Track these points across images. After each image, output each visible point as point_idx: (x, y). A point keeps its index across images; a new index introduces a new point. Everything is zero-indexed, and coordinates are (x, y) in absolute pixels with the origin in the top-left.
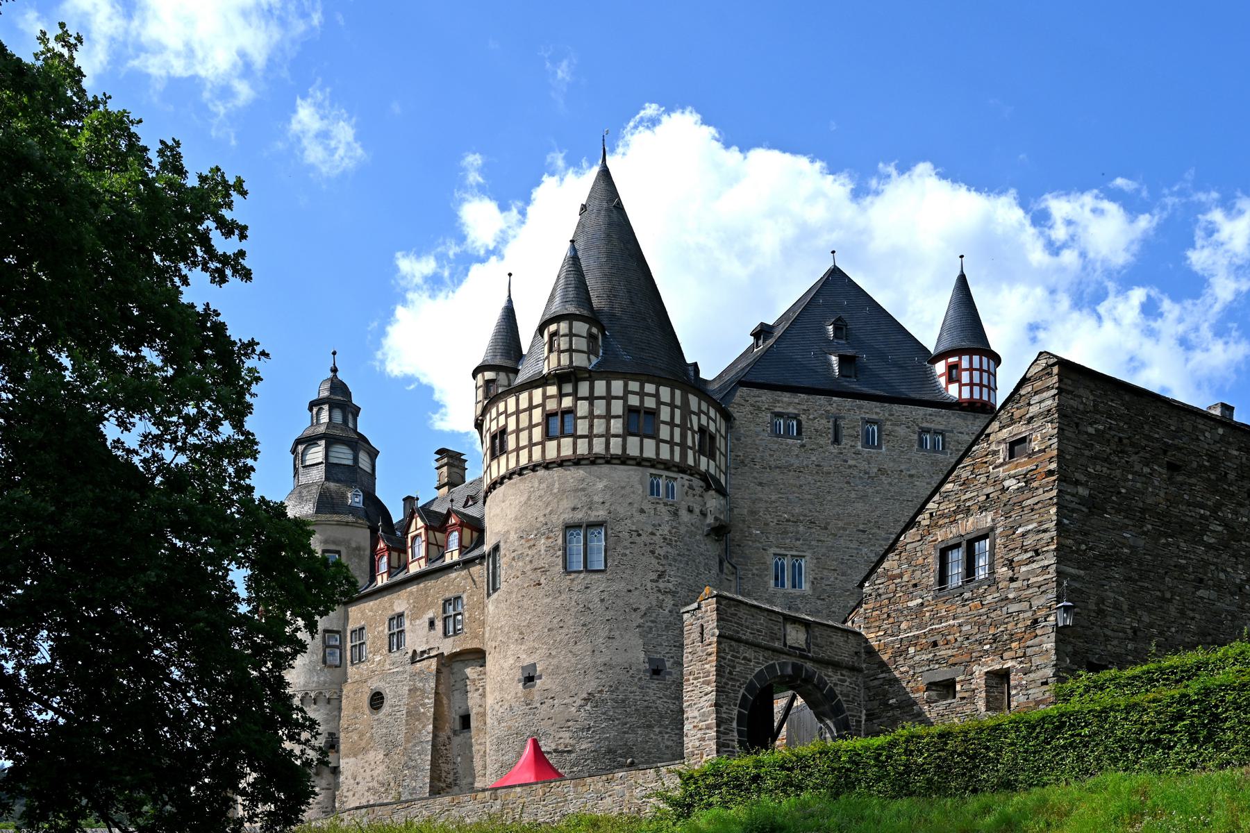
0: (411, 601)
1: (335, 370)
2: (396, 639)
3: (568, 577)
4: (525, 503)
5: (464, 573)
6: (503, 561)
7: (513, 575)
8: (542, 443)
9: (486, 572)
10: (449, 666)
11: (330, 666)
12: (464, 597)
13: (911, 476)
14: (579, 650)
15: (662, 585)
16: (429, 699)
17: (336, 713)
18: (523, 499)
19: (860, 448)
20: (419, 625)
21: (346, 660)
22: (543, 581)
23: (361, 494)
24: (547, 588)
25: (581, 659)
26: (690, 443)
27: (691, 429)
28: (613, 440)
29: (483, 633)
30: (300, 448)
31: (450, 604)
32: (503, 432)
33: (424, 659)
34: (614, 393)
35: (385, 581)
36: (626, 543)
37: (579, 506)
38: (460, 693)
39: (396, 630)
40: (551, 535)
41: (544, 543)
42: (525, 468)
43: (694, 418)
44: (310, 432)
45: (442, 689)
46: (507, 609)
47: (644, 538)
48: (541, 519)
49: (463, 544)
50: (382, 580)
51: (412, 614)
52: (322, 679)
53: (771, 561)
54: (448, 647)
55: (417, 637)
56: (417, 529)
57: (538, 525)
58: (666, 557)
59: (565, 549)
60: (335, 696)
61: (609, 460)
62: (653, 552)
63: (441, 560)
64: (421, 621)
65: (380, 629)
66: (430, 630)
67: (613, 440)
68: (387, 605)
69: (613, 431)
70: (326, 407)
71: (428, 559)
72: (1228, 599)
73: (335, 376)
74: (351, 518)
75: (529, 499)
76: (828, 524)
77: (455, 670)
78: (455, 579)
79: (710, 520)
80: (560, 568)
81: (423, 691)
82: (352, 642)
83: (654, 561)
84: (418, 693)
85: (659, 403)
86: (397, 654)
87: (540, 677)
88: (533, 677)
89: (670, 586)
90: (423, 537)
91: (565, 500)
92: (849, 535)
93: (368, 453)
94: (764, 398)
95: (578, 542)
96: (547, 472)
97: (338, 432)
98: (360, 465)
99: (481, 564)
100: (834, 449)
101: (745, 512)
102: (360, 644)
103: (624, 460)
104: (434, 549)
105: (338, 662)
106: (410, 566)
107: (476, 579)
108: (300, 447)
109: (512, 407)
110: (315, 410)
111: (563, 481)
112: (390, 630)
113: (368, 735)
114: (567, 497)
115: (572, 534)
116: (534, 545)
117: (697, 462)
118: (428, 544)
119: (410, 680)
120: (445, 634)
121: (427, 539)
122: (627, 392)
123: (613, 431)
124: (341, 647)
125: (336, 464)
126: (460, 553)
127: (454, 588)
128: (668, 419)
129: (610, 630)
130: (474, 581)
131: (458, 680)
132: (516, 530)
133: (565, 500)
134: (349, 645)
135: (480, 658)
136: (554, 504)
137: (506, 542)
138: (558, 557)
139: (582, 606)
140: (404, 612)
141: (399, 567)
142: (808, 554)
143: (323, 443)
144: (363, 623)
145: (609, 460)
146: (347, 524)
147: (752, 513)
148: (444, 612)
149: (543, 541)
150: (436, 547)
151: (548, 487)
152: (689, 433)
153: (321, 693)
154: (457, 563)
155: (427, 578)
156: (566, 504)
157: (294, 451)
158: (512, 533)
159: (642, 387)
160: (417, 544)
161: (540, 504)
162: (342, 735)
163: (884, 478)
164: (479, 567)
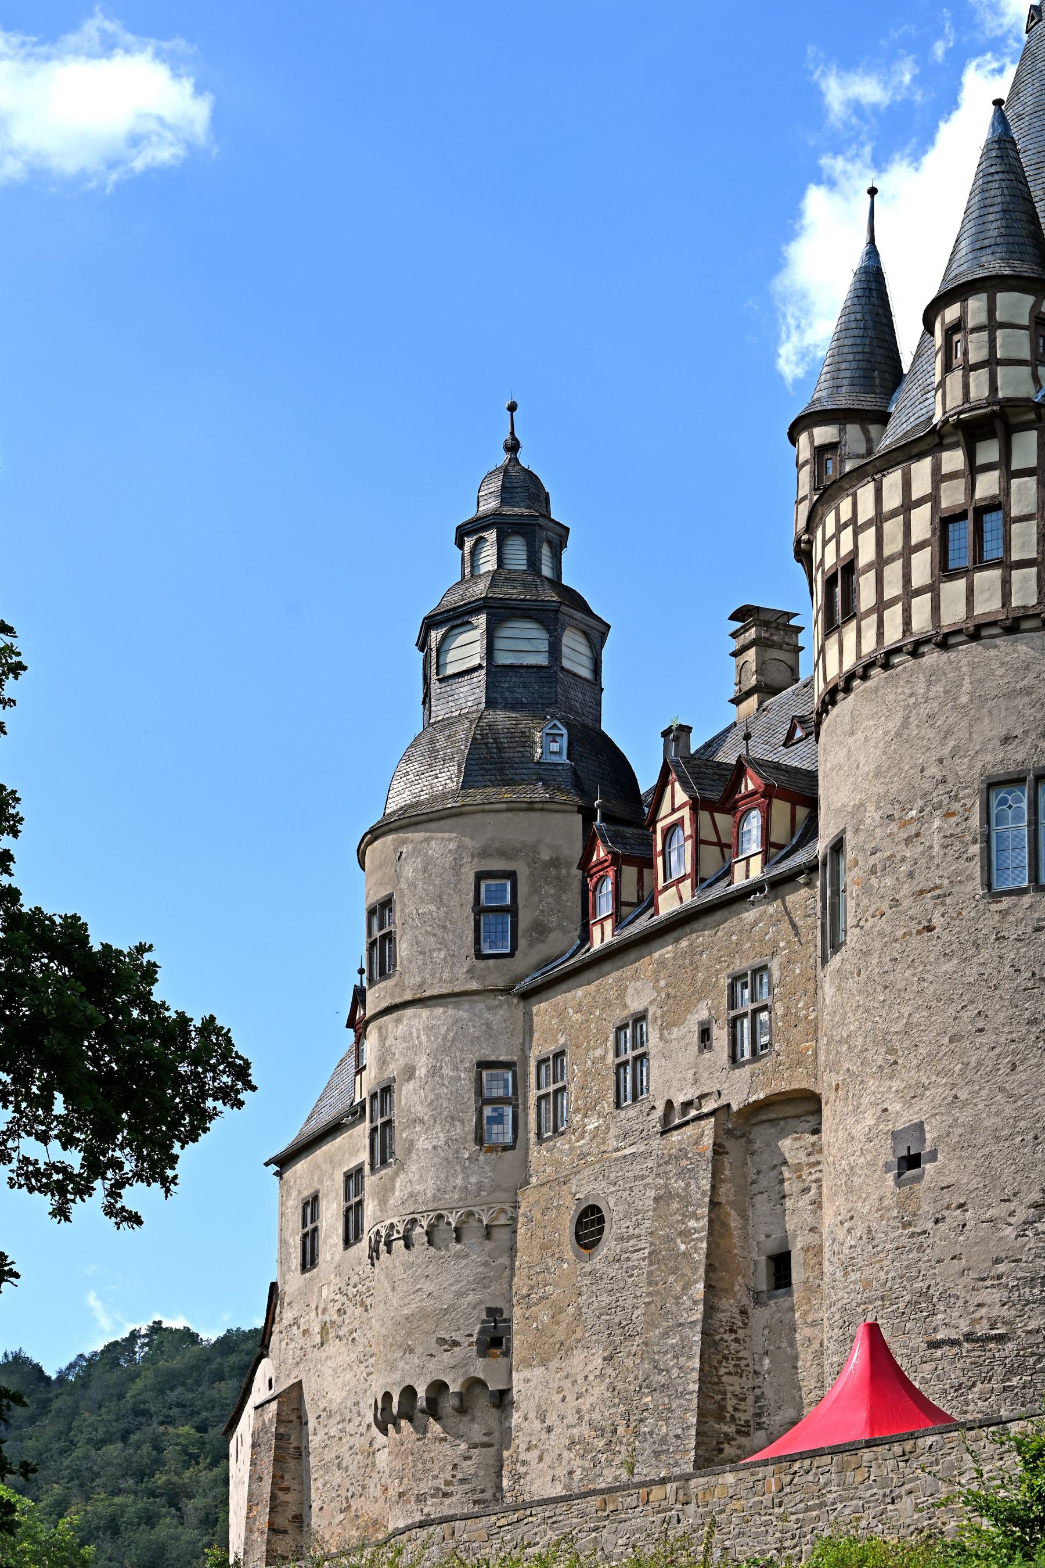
0: (662, 983)
1: (513, 447)
3: (994, 907)
4: (898, 734)
5: (773, 908)
6: (850, 878)
7: (872, 909)
8: (933, 589)
9: (819, 905)
10: (743, 1135)
11: (491, 1149)
12: (775, 965)
14: (1021, 1084)
16: (698, 1219)
17: (504, 1260)
18: (893, 725)
20: (678, 1040)
21: (527, 1131)
22: (937, 921)
23: (564, 731)
24: (946, 936)
25: (1027, 1107)
29: (816, 1053)
30: (435, 636)
31: (745, 986)
32: (849, 568)
33: (687, 1123)
35: (608, 938)
37: (1019, 732)
38: (769, 1201)
39: (630, 1054)
40: (956, 806)
41: (940, 829)
42: (897, 651)
44: (455, 599)
45: (726, 1191)
46: (860, 992)
48: (933, 770)
49: (773, 839)
50: (603, 936)
51: (664, 1014)
52: (473, 1180)
56: (674, 810)
57: (927, 785)
59: (987, 840)
60: (503, 1220)
63: (725, 882)
64: (684, 1030)
65: (598, 1052)
66: (701, 1051)
68: (612, 994)
70: (491, 536)
71: (699, 881)
73: (515, 461)
74: (540, 793)
75: (906, 723)
77: (757, 1146)
78: (755, 923)
81: (686, 1200)
82: (539, 1088)
84: (675, 1206)
86: (632, 1113)
87: (933, 1156)
88: (918, 1155)
90: (688, 830)
91: (987, 721)
93: (584, 633)
95: (1018, 818)
96: (945, 656)
97: (515, 592)
98: (566, 664)
99: (809, 884)
102: (556, 1092)
104: (710, 854)
105: (508, 1138)
106: (661, 899)
107: (799, 923)
108: (433, 633)
109: (866, 511)
110: (469, 543)
111: (980, 673)
112: (617, 1054)
113: (571, 1310)
114: (990, 712)
115: (1003, 801)
116: (918, 835)
118: (698, 842)
119: (658, 1175)
120: (734, 1059)
121: (697, 831)
124: (514, 1101)
125: (512, 667)
126: (765, 862)
127: (752, 947)
130: (794, 926)
131: (764, 1167)
132: (878, 802)
133: (987, 721)
134: (533, 1094)
135: (812, 1113)
136: (961, 733)
137: (857, 831)
138: (970, 859)
139: (1029, 974)
140: (646, 1010)
141: (640, 900)
143: (481, 620)
144: (562, 1041)
146: (531, 807)
148: (732, 1005)
149: (937, 823)
150: (717, 848)
151: (946, 692)
153: (471, 1214)
154: (756, 888)
155: (696, 925)
156: (989, 729)
157: (423, 644)
158: (871, 807)
160: (674, 845)
161: (931, 733)
162: (517, 1311)
164: (804, 892)
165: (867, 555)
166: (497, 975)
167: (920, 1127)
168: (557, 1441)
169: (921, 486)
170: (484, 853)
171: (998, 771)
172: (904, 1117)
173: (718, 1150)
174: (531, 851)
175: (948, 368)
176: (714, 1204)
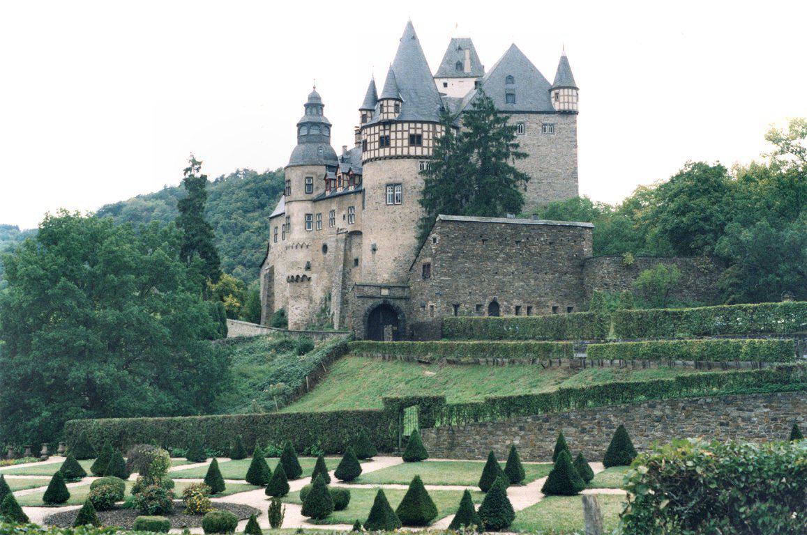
2: (333, 220)
13: (539, 146)
28: (404, 148)
47: (417, 189)
54: (350, 228)
61: (403, 157)
67: (404, 148)
69: (404, 145)
80: (384, 203)
85: (423, 131)
103: (409, 157)
122: (409, 128)
123: (404, 145)
128: (427, 137)
145: (403, 157)
159: (416, 125)
165: (368, 141)
166: (309, 197)
169: (377, 131)
170: (307, 173)
173: (346, 239)
174: (316, 173)
175: (381, 112)
176: (345, 250)
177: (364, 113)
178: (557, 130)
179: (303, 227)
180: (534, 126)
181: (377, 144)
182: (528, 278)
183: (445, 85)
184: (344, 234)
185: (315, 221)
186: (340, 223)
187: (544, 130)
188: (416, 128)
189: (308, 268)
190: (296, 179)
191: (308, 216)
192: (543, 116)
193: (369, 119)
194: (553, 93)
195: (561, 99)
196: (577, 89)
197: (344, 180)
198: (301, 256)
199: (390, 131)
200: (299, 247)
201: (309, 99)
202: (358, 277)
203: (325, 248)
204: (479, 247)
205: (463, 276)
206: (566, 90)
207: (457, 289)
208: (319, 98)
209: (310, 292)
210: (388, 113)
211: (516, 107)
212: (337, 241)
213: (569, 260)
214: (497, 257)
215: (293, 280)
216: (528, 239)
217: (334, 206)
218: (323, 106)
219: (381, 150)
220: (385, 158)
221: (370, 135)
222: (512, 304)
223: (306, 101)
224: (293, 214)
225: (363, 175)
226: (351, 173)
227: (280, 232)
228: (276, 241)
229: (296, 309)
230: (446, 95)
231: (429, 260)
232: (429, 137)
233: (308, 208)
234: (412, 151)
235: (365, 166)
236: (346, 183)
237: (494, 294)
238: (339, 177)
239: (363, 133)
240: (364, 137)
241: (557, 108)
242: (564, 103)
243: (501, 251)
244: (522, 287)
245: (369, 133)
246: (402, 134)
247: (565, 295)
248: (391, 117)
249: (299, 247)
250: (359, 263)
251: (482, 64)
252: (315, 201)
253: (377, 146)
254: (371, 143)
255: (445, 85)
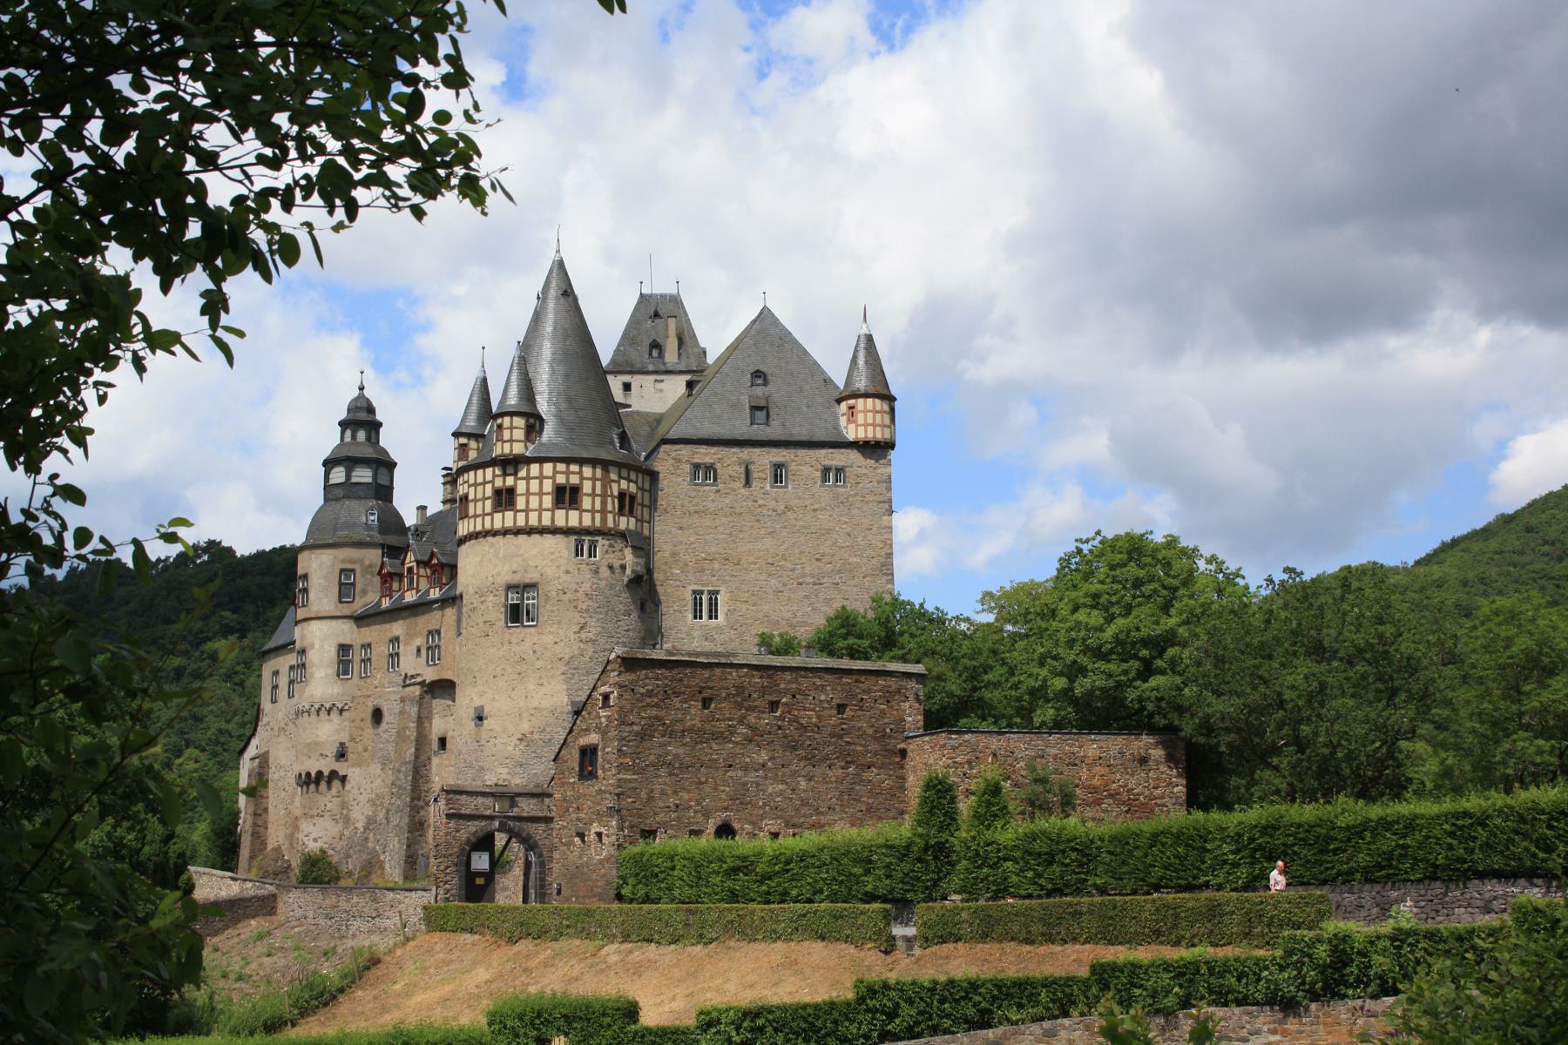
13: (815, 510)
15: (583, 636)
19: (768, 487)
26: (610, 508)
27: (612, 496)
28: (544, 513)
34: (545, 474)
36: (554, 601)
43: (615, 486)
47: (568, 595)
48: (490, 579)
53: (689, 597)
54: (430, 675)
55: (410, 663)
58: (587, 611)
61: (542, 531)
62: (576, 607)
67: (544, 513)
69: (544, 506)
72: (753, 774)
76: (740, 560)
79: (628, 571)
83: (577, 615)
85: (582, 479)
89: (591, 635)
92: (759, 569)
94: (684, 452)
100: (745, 492)
101: (667, 554)
103: (554, 531)
117: (616, 523)
122: (555, 472)
123: (544, 506)
129: (540, 678)
142: (723, 590)
145: (542, 531)
147: (673, 554)
152: (609, 499)
154: (435, 601)
159: (568, 468)
163: (789, 514)
165: (471, 497)
167: (482, 707)
168: (364, 799)
169: (489, 477)
170: (344, 561)
171: (512, 583)
172: (478, 703)
173: (422, 697)
174: (360, 562)
176: (419, 717)
177: (463, 440)
178: (851, 480)
179: (332, 670)
180: (806, 470)
181: (489, 503)
182: (795, 774)
183: (627, 387)
184: (418, 687)
185: (357, 659)
186: (410, 663)
187: (825, 479)
188: (568, 473)
189: (341, 755)
190: (319, 570)
191: (344, 649)
192: (823, 452)
193: (472, 455)
194: (844, 406)
195: (860, 418)
196: (890, 399)
197: (419, 576)
198: (328, 731)
199: (517, 479)
200: (323, 713)
201: (349, 410)
202: (443, 772)
203: (377, 715)
204: (694, 714)
205: (663, 772)
206: (870, 400)
207: (650, 799)
208: (371, 410)
209: (344, 805)
210: (511, 441)
211: (774, 431)
212: (403, 700)
213: (875, 739)
214: (732, 734)
215: (310, 781)
216: (794, 696)
217: (398, 628)
218: (380, 425)
219: (498, 516)
220: (505, 532)
221: (476, 485)
222: (761, 829)
223: (343, 415)
224: (312, 646)
225: (460, 565)
226: (435, 561)
227: (283, 681)
228: (274, 701)
229: (315, 840)
230: (629, 406)
231: (593, 738)
232: (594, 489)
233: (346, 632)
234: (560, 518)
235: (464, 549)
236: (424, 584)
237: (726, 809)
238: (410, 570)
239: (460, 480)
240: (462, 490)
241: (851, 437)
242: (866, 425)
243: (741, 720)
244: (781, 793)
245: (472, 481)
246: (541, 484)
247: (869, 810)
248: (518, 449)
249: (323, 713)
250: (448, 746)
251: (702, 345)
252: (361, 620)
253: (488, 508)
254: (476, 500)
255: (627, 387)
